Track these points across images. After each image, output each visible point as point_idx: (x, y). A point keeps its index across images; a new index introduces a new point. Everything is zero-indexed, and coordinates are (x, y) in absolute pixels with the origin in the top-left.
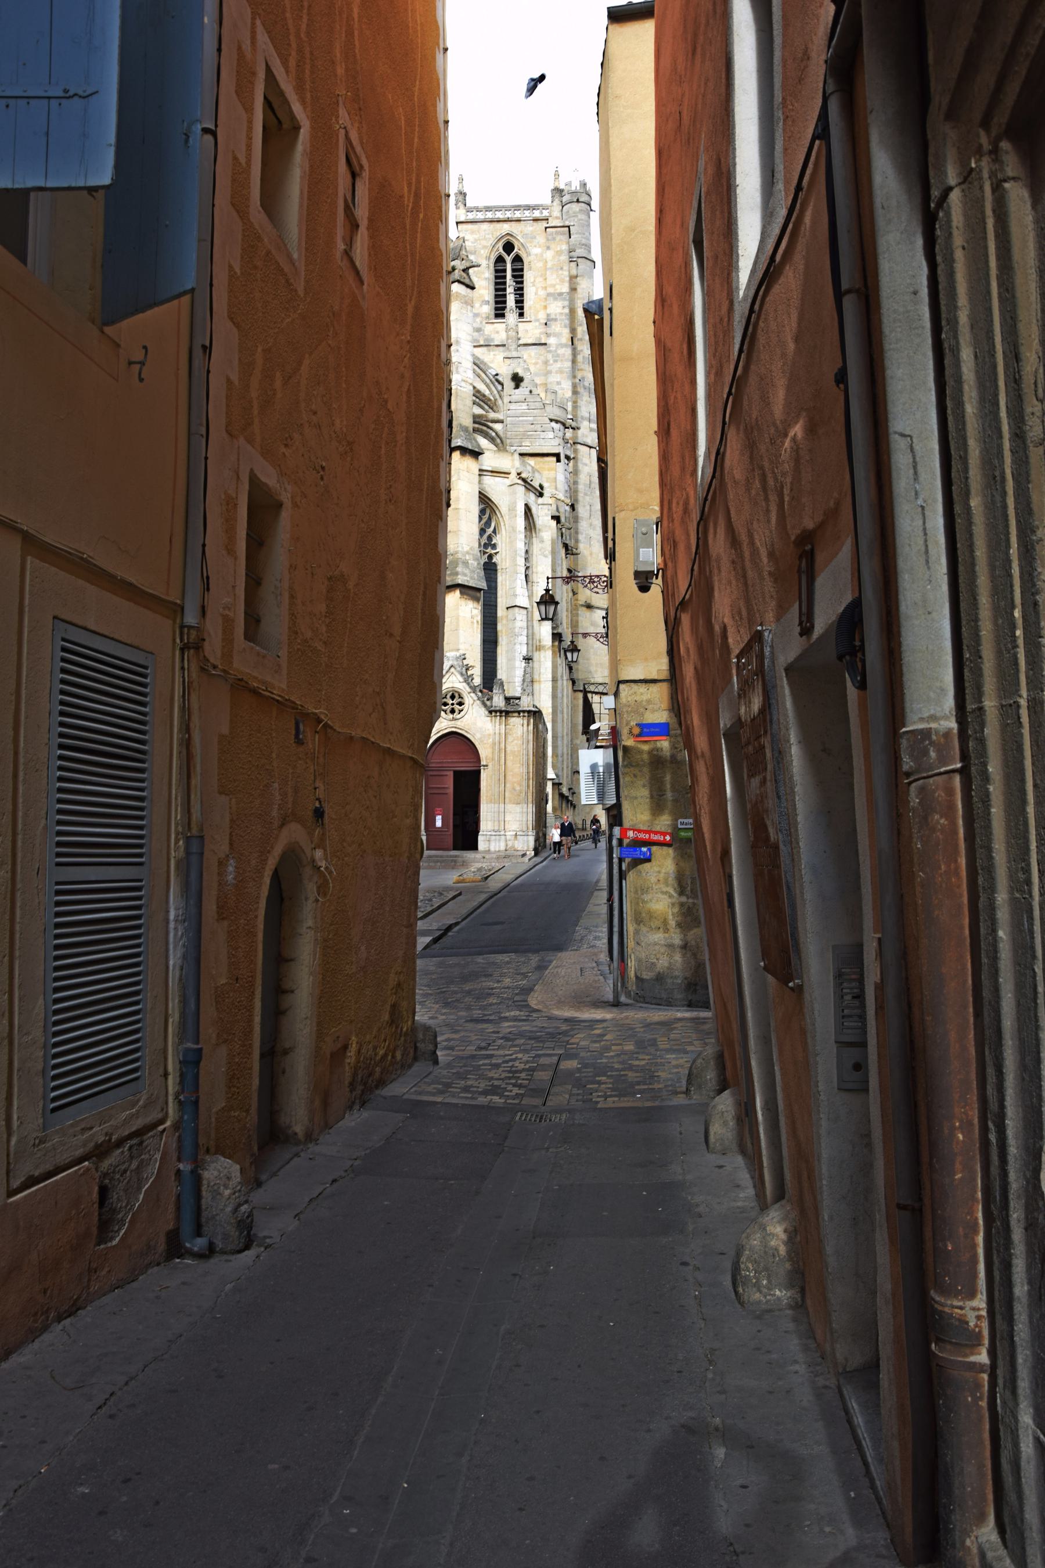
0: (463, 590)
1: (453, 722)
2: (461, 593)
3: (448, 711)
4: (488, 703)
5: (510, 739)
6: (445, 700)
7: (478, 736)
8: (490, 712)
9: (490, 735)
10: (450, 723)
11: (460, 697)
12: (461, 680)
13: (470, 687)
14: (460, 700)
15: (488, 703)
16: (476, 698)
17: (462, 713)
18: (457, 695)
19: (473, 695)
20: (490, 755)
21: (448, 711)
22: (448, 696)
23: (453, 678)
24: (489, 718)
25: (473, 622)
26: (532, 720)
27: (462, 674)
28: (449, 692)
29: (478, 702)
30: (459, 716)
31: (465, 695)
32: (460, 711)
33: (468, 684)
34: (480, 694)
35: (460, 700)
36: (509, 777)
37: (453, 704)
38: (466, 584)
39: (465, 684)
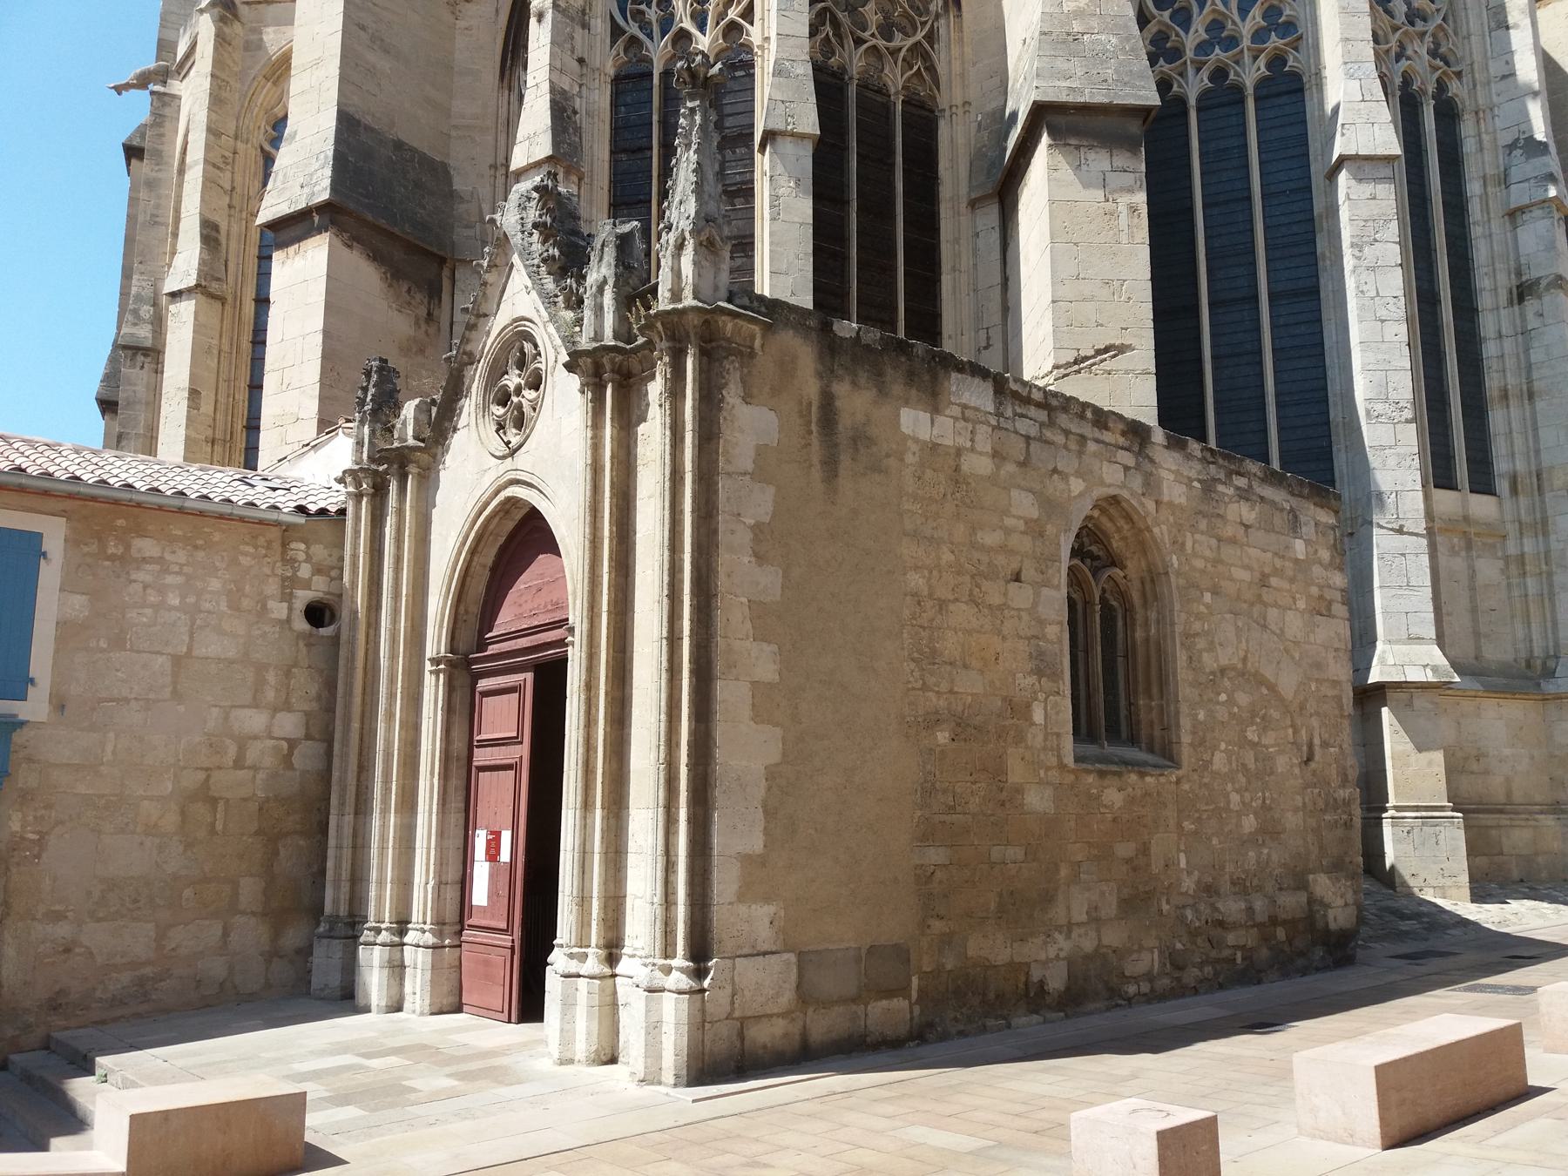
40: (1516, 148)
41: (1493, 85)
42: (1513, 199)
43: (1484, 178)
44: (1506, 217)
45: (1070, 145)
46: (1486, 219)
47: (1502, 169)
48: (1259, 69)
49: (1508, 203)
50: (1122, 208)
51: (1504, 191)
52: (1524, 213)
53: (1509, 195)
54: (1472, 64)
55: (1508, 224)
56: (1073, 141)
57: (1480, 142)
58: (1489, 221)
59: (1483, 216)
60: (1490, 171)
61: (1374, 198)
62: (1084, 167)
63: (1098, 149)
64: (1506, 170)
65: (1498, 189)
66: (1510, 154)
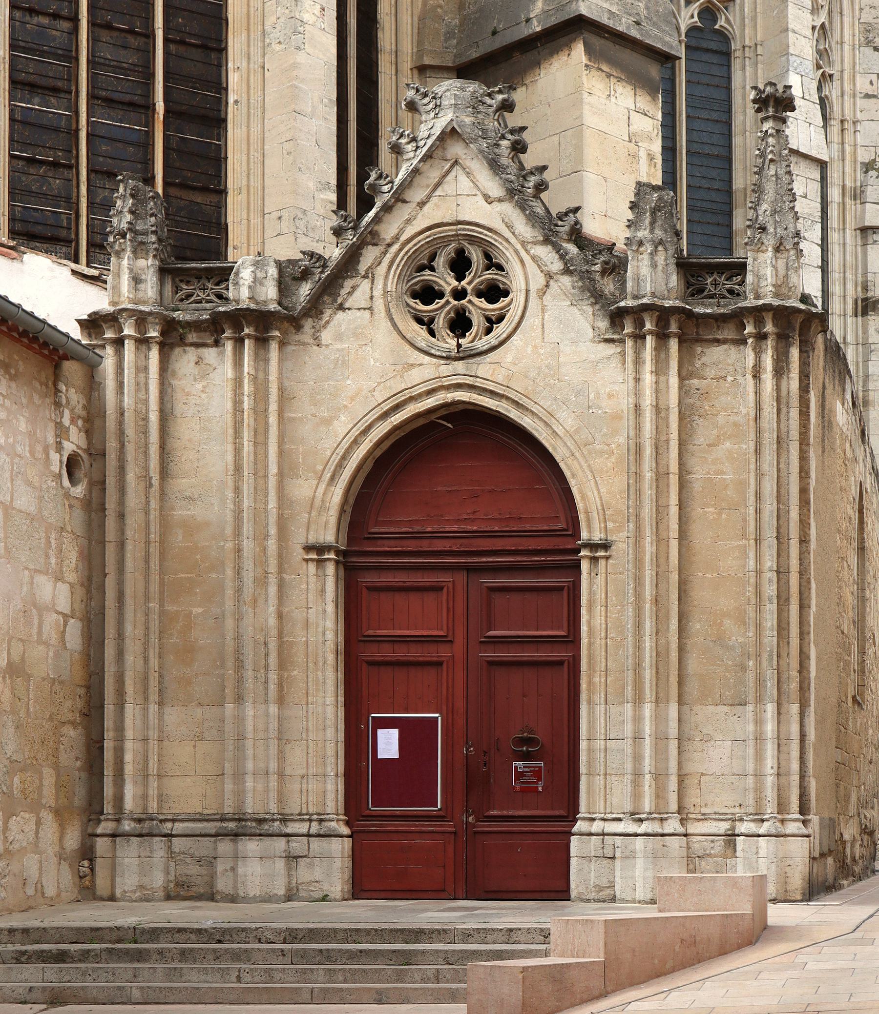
0: (597, 42)
1: (459, 366)
2: (589, 51)
3: (440, 323)
4: (608, 286)
5: (703, 434)
6: (427, 275)
7: (566, 420)
8: (617, 317)
9: (616, 417)
10: (446, 369)
11: (491, 263)
12: (495, 189)
13: (532, 218)
14: (490, 275)
15: (608, 286)
16: (557, 266)
17: (501, 330)
18: (475, 255)
19: (545, 253)
20: (619, 503)
21: (440, 323)
22: (441, 262)
23: (459, 182)
24: (611, 350)
25: (634, 156)
26: (795, 353)
27: (495, 165)
28: (445, 241)
29: (566, 281)
30: (483, 343)
31: (509, 256)
32: (492, 322)
33: (522, 206)
34: (572, 249)
35: (490, 275)
36: (701, 595)
37: (459, 294)
38: (605, 20)
39: (508, 209)
40: (873, 169)
41: (858, 100)
42: (868, 216)
43: (844, 187)
44: (858, 232)
45: (603, 71)
46: (841, 227)
47: (859, 184)
48: (692, 16)
49: (863, 218)
50: (643, 154)
51: (859, 206)
52: (874, 233)
53: (864, 211)
54: (842, 72)
55: (859, 238)
56: (605, 67)
57: (843, 151)
58: (844, 229)
59: (839, 224)
60: (849, 184)
61: (806, 197)
62: (613, 99)
63: (625, 84)
64: (861, 186)
65: (853, 203)
66: (866, 172)
